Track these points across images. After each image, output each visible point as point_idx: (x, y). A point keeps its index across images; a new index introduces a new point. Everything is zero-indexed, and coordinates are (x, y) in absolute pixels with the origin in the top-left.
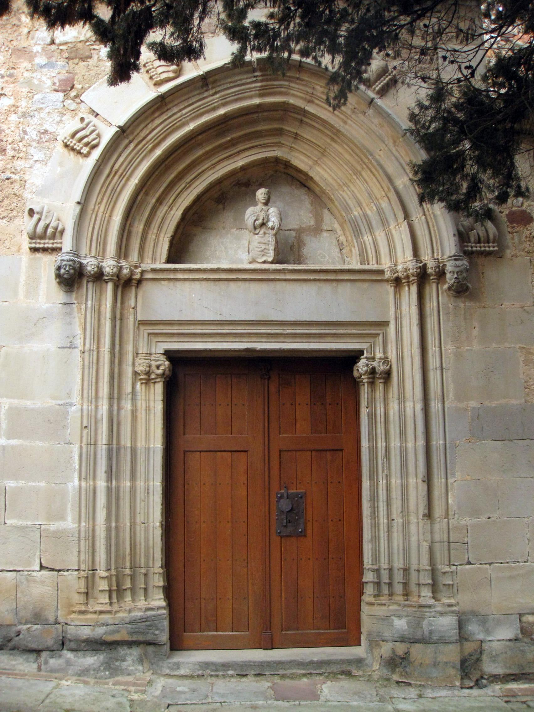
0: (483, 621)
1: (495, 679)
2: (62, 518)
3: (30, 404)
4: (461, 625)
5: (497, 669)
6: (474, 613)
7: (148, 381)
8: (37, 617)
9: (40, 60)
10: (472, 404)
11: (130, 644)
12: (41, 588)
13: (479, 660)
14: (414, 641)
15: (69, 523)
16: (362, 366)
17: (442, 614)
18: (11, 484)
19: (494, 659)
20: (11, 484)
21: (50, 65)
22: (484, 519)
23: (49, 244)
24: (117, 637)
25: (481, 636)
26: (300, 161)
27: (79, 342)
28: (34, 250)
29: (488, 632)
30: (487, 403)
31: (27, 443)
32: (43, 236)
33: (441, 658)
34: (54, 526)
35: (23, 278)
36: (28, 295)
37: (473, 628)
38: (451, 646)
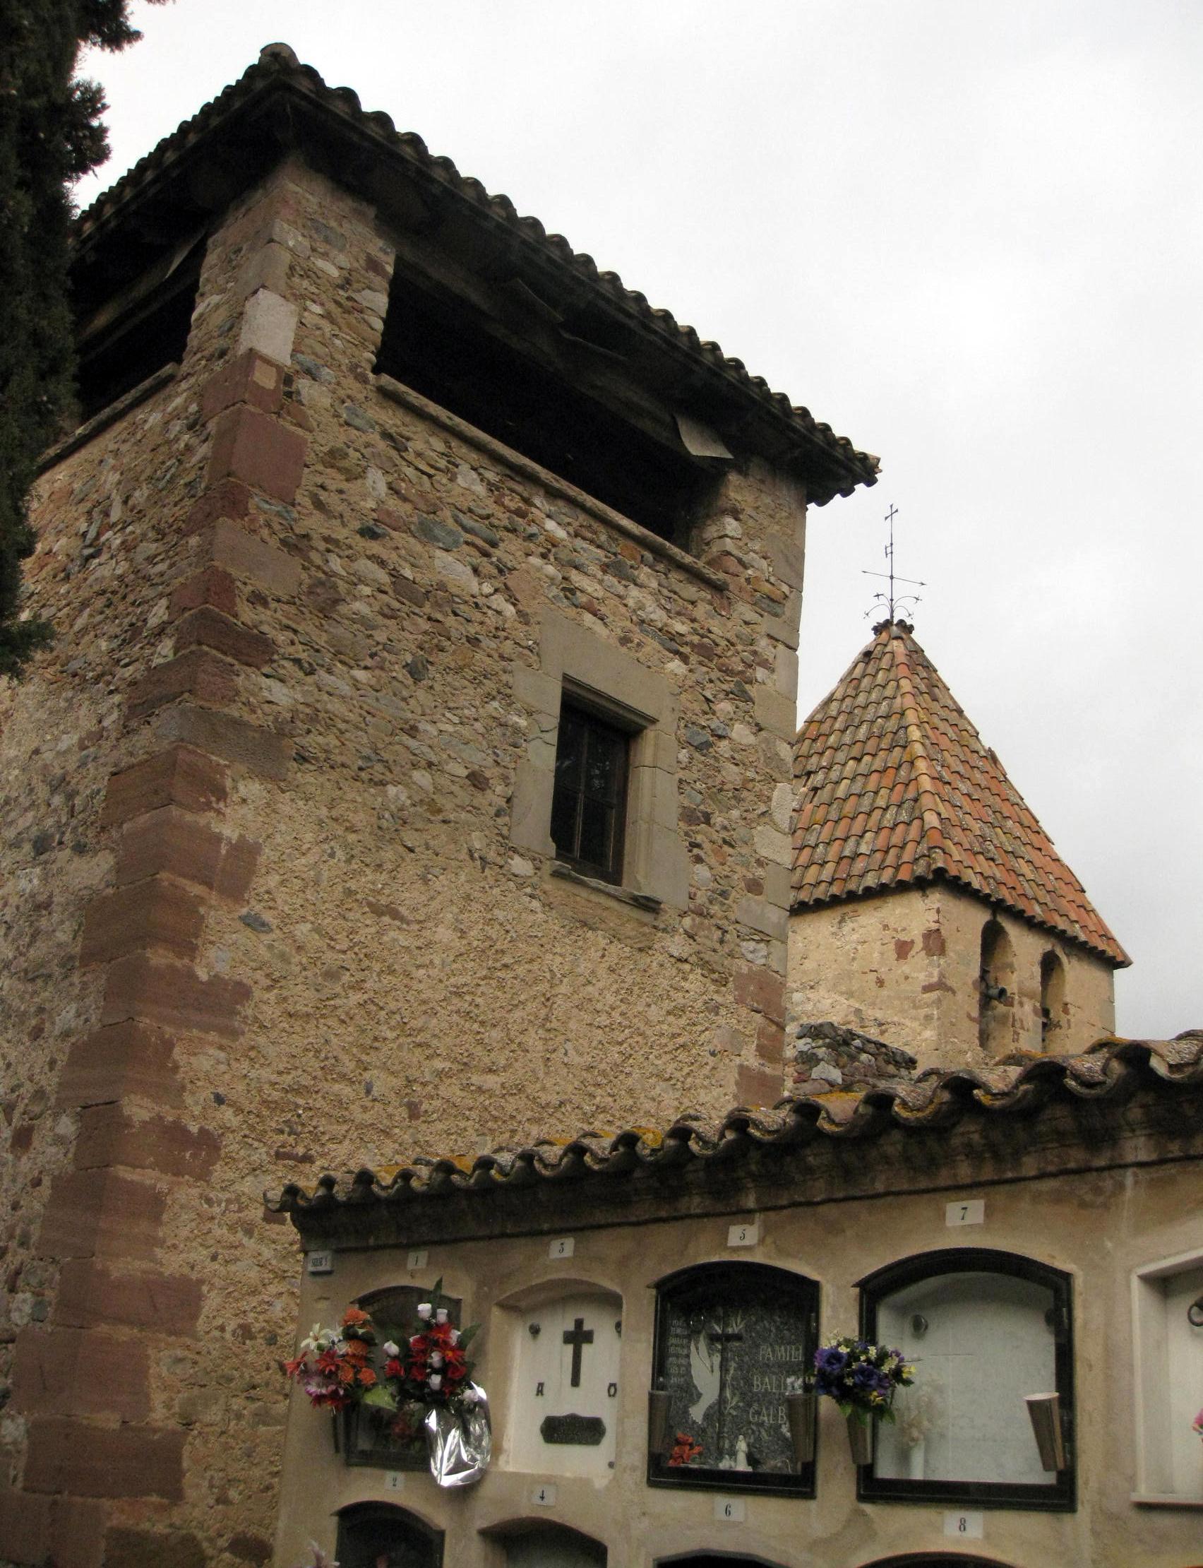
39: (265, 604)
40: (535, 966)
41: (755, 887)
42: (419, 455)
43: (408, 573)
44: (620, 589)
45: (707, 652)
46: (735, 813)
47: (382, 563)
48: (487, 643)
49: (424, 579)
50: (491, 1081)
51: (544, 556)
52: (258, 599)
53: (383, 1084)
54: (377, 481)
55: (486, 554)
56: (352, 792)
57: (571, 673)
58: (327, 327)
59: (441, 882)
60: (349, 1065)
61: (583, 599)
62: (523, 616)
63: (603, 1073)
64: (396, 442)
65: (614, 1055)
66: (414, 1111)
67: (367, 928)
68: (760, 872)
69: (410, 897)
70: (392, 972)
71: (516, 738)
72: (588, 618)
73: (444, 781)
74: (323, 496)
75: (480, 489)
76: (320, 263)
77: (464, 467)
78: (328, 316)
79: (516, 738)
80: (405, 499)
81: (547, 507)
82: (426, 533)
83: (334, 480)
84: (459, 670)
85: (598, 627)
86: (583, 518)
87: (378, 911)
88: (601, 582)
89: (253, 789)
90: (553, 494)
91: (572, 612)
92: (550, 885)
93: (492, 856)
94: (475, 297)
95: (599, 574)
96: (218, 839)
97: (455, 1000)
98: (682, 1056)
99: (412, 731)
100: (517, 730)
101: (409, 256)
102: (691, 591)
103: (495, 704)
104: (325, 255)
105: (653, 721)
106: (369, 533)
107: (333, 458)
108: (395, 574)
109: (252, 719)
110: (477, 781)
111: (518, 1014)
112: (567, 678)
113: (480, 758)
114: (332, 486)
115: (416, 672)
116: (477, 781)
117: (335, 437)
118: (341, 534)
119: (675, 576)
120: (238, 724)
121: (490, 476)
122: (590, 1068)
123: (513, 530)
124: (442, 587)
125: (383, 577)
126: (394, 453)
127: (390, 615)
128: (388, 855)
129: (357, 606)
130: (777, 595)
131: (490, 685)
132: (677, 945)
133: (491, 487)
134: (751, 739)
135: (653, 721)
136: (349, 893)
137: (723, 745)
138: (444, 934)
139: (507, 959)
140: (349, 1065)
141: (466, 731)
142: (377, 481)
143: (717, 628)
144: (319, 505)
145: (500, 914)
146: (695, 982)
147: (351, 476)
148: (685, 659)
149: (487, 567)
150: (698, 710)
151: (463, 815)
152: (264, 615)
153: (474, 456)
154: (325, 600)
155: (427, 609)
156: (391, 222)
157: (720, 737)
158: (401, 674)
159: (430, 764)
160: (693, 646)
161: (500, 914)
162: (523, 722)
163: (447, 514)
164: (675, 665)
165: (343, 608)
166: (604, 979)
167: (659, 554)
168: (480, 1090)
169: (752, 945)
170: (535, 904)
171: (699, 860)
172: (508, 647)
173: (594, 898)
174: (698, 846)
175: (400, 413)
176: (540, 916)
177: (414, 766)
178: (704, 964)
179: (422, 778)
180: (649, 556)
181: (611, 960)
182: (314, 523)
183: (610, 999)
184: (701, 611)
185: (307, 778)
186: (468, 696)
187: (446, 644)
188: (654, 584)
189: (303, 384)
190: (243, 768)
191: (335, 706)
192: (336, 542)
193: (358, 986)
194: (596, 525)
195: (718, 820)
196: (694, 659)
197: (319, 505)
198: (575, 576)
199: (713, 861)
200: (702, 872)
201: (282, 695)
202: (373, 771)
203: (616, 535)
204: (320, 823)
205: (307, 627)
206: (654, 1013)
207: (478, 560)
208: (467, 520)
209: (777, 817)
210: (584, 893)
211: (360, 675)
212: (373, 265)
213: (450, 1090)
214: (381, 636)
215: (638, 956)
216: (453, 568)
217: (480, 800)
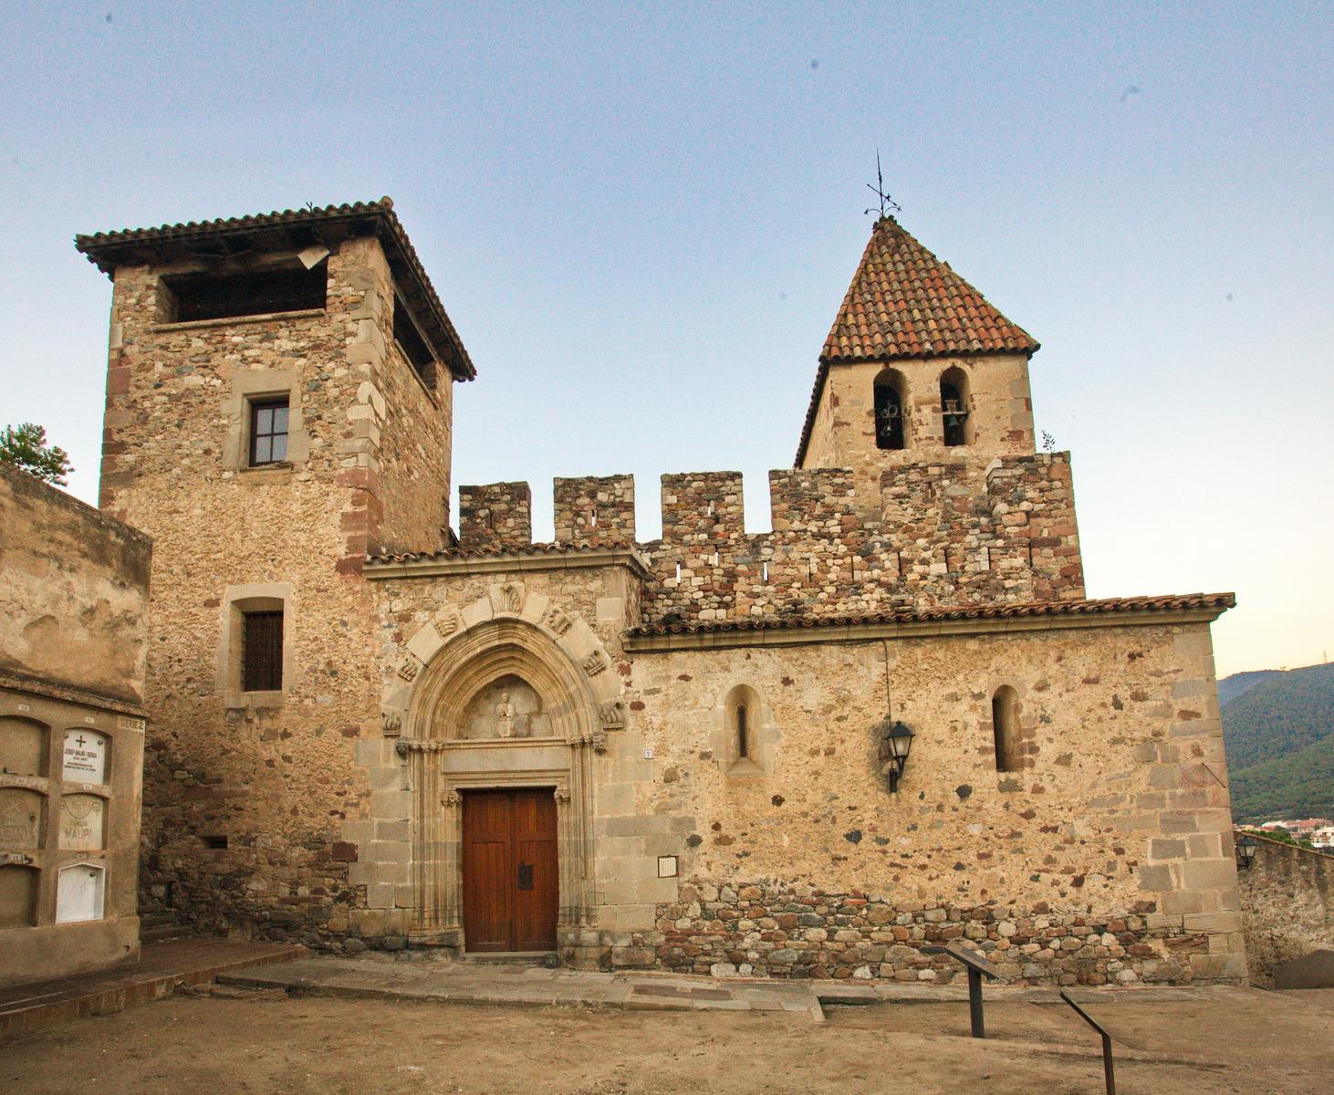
0: (612, 936)
1: (619, 967)
2: (405, 881)
3: (389, 821)
4: (601, 937)
5: (619, 962)
6: (607, 932)
7: (449, 804)
8: (394, 933)
9: (385, 623)
10: (607, 816)
11: (440, 947)
12: (396, 918)
13: (610, 957)
14: (576, 946)
15: (408, 883)
16: (556, 795)
17: (590, 931)
18: (380, 863)
19: (617, 956)
20: (380, 863)
21: (390, 626)
22: (613, 880)
23: (393, 733)
24: (432, 943)
25: (611, 944)
26: (525, 676)
27: (411, 787)
28: (387, 736)
29: (615, 942)
30: (615, 816)
31: (387, 842)
32: (391, 729)
33: (590, 955)
34: (401, 885)
35: (382, 750)
36: (385, 762)
37: (607, 940)
38: (594, 949)
39: (122, 431)
40: (236, 509)
41: (348, 435)
42: (175, 346)
43: (174, 392)
44: (269, 345)
45: (316, 347)
46: (336, 409)
47: (164, 394)
48: (208, 400)
49: (182, 390)
50: (219, 555)
51: (231, 353)
52: (121, 431)
53: (176, 569)
54: (159, 366)
55: (205, 367)
56: (159, 478)
57: (246, 391)
58: (133, 323)
59: (196, 495)
60: (164, 567)
61: (251, 359)
62: (224, 382)
63: (269, 538)
64: (165, 348)
65: (274, 529)
66: (189, 575)
67: (166, 521)
68: (351, 427)
69: (182, 503)
70: (177, 531)
71: (223, 429)
72: (254, 366)
73: (195, 458)
74: (138, 383)
75: (201, 343)
76: (128, 301)
77: (194, 340)
78: (134, 319)
79: (223, 429)
80: (170, 366)
81: (233, 332)
82: (180, 373)
83: (141, 375)
84: (197, 416)
85: (260, 367)
86: (248, 326)
87: (170, 513)
88: (259, 348)
89: (123, 492)
90: (233, 325)
91: (246, 367)
92: (240, 476)
93: (214, 476)
94: (197, 269)
95: (258, 345)
96: (113, 512)
97: (204, 532)
98: (309, 519)
99: (179, 447)
100: (224, 425)
101: (167, 271)
102: (308, 325)
103: (215, 421)
104: (131, 297)
105: (289, 391)
106: (158, 386)
107: (142, 368)
108: (169, 396)
109: (122, 470)
110: (207, 452)
111: (229, 529)
112: (245, 395)
113: (206, 444)
114: (140, 378)
115: (179, 426)
116: (207, 452)
117: (141, 359)
118: (146, 392)
119: (298, 323)
120: (119, 473)
121: (206, 335)
122: (262, 538)
123: (216, 351)
124: (188, 389)
125: (165, 398)
126: (164, 352)
127: (170, 410)
128: (173, 493)
129: (156, 414)
130: (358, 298)
131: (211, 415)
132: (303, 477)
133: (205, 340)
134: (346, 372)
135: (289, 391)
136: (160, 511)
137: (330, 383)
138: (197, 511)
139: (224, 510)
140: (164, 567)
141: (201, 437)
142: (159, 366)
143: (322, 334)
144: (138, 387)
145: (219, 496)
146: (315, 488)
147: (148, 370)
148: (304, 356)
149: (207, 371)
150: (313, 374)
151: (203, 467)
152: (123, 434)
153: (192, 333)
154: (144, 418)
155: (183, 401)
156: (153, 265)
157: (326, 380)
158: (174, 429)
159: (187, 455)
160: (309, 349)
161: (219, 496)
162: (225, 422)
163: (187, 362)
164: (302, 361)
165: (150, 418)
166: (268, 501)
167: (284, 319)
168: (215, 560)
169: (346, 461)
170: (235, 486)
171: (315, 436)
172: (218, 398)
173: (261, 473)
174: (314, 431)
175: (166, 336)
176: (237, 490)
177: (182, 458)
178: (318, 478)
179: (186, 462)
180: (283, 323)
181: (272, 493)
182: (137, 395)
183: (271, 508)
184: (313, 333)
185: (142, 481)
186: (202, 424)
187: (191, 409)
188: (287, 333)
189: (128, 350)
190: (118, 487)
191: (152, 452)
192: (146, 397)
193: (165, 541)
194: (253, 326)
195: (325, 417)
196: (310, 354)
197: (138, 387)
198: (247, 353)
199: (322, 434)
200: (318, 442)
201: (130, 458)
202: (165, 469)
203: (265, 324)
204: (147, 493)
205: (139, 431)
206: (294, 507)
207: (202, 370)
208: (194, 359)
209: (360, 400)
210: (256, 473)
211: (158, 437)
212: (149, 287)
213: (204, 563)
214: (165, 420)
215: (284, 487)
216: (194, 380)
217: (209, 458)
